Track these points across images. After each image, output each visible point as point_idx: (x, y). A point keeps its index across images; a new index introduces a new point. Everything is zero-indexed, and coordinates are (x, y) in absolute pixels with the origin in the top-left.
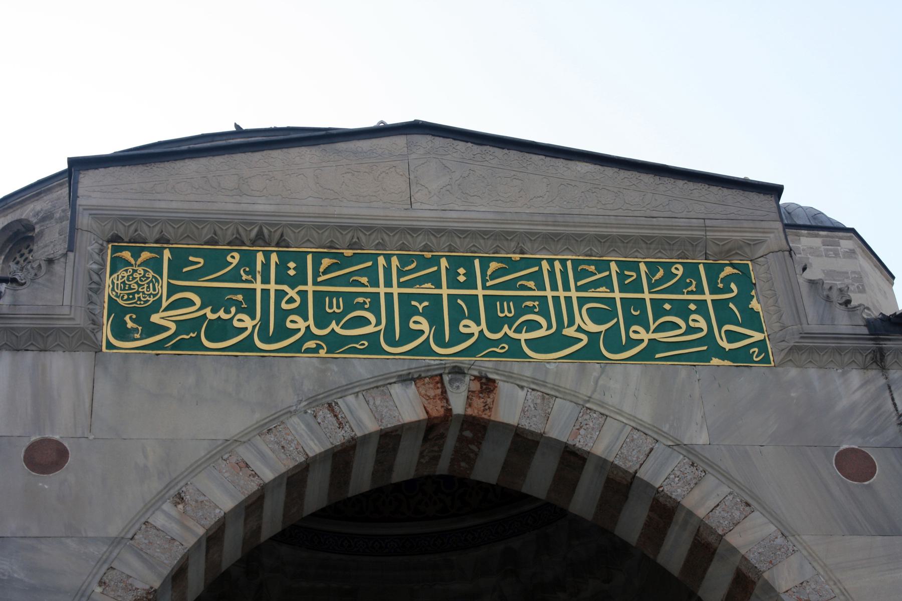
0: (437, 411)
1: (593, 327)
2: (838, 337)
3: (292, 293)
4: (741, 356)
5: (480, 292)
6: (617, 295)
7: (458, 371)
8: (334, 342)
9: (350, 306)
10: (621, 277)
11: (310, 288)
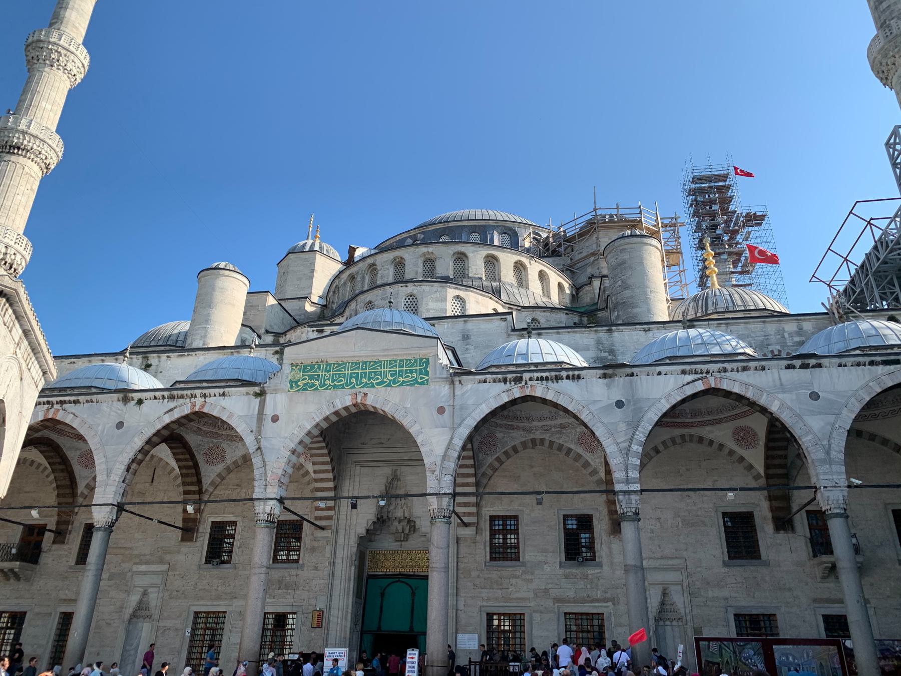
0: (354, 402)
4: (422, 384)
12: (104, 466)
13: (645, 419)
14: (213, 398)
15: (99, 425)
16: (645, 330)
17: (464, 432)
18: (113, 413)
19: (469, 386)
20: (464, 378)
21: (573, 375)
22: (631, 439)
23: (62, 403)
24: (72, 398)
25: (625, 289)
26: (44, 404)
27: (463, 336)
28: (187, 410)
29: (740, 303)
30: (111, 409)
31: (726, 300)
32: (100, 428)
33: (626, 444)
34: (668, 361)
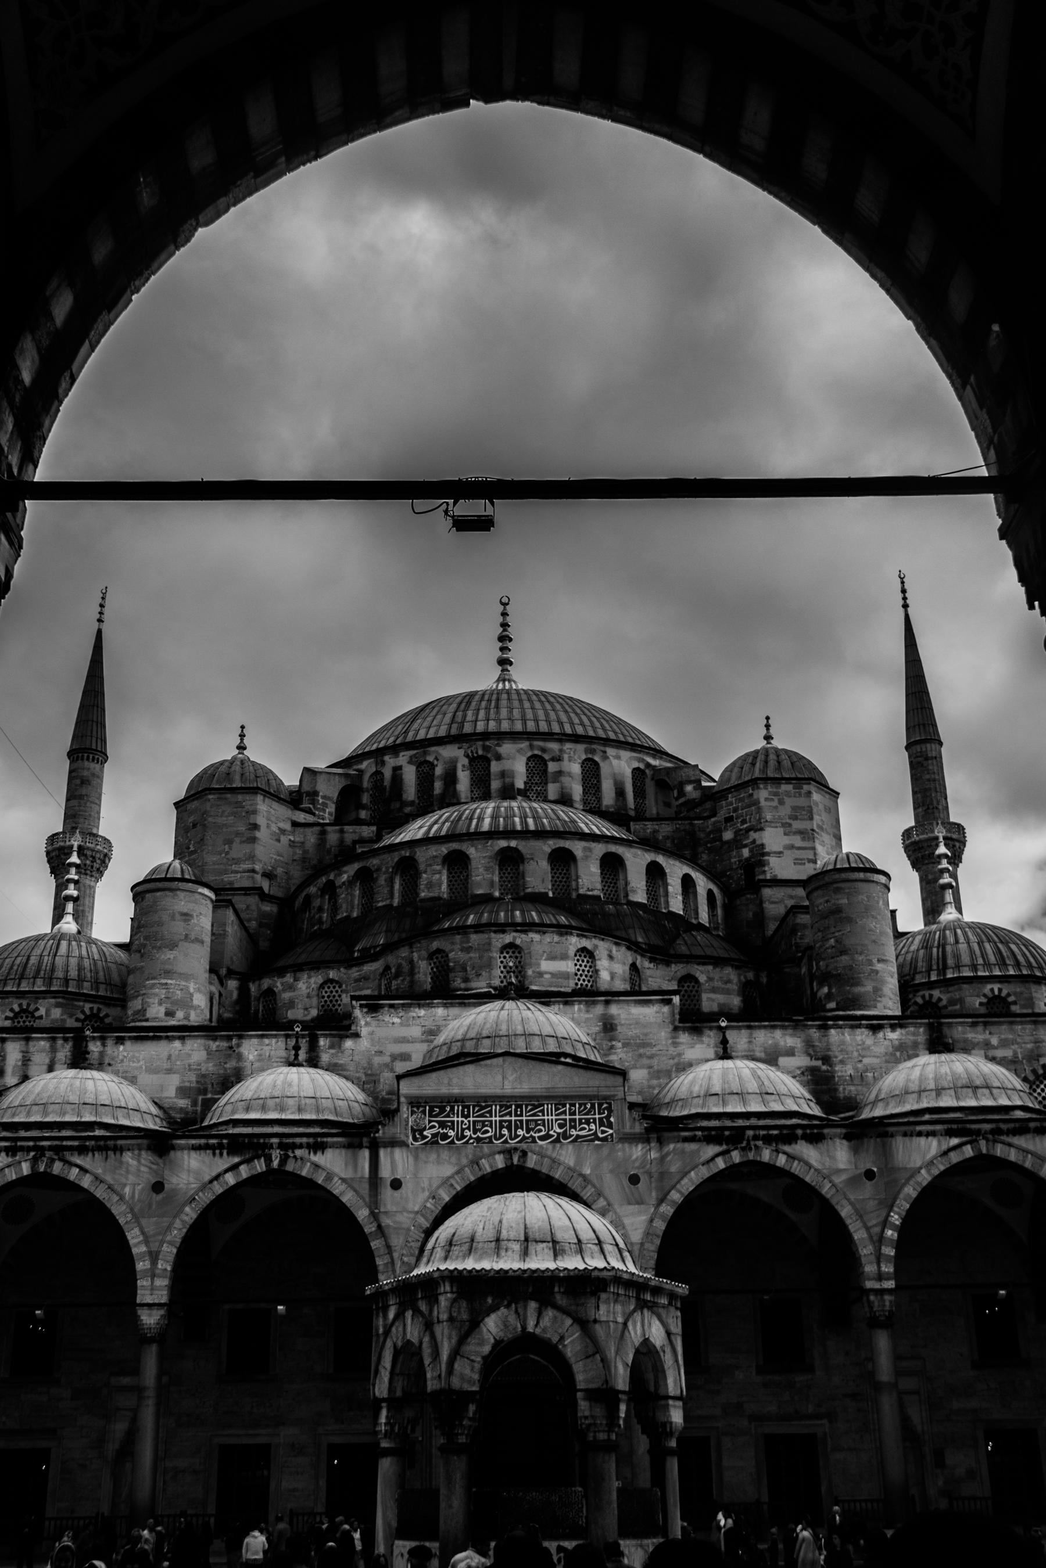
0: (509, 1164)
1: (559, 1130)
2: (634, 1134)
3: (466, 1121)
5: (524, 1118)
6: (568, 1117)
7: (516, 1149)
8: (479, 1140)
9: (484, 1126)
10: (570, 1109)
11: (471, 1119)
12: (143, 1248)
13: (901, 1196)
14: (299, 1153)
15: (125, 1185)
16: (875, 1029)
17: (667, 1210)
18: (143, 1169)
19: (672, 1146)
20: (666, 1135)
21: (812, 1134)
22: (885, 1223)
23: (58, 1150)
24: (76, 1143)
25: (843, 952)
26: (29, 1149)
27: (605, 1025)
28: (260, 1166)
29: (992, 959)
30: (139, 1161)
31: (972, 952)
32: (127, 1190)
33: (877, 1230)
34: (927, 1117)
